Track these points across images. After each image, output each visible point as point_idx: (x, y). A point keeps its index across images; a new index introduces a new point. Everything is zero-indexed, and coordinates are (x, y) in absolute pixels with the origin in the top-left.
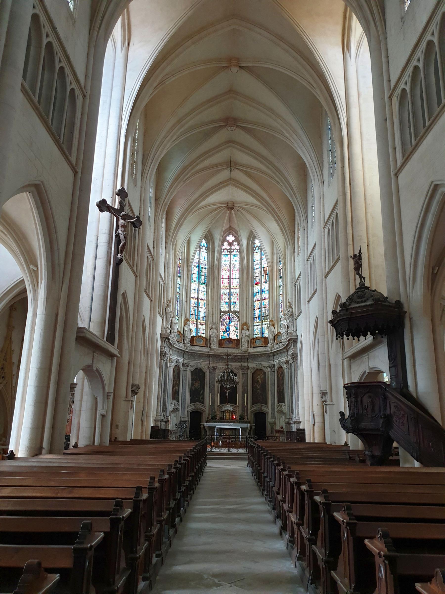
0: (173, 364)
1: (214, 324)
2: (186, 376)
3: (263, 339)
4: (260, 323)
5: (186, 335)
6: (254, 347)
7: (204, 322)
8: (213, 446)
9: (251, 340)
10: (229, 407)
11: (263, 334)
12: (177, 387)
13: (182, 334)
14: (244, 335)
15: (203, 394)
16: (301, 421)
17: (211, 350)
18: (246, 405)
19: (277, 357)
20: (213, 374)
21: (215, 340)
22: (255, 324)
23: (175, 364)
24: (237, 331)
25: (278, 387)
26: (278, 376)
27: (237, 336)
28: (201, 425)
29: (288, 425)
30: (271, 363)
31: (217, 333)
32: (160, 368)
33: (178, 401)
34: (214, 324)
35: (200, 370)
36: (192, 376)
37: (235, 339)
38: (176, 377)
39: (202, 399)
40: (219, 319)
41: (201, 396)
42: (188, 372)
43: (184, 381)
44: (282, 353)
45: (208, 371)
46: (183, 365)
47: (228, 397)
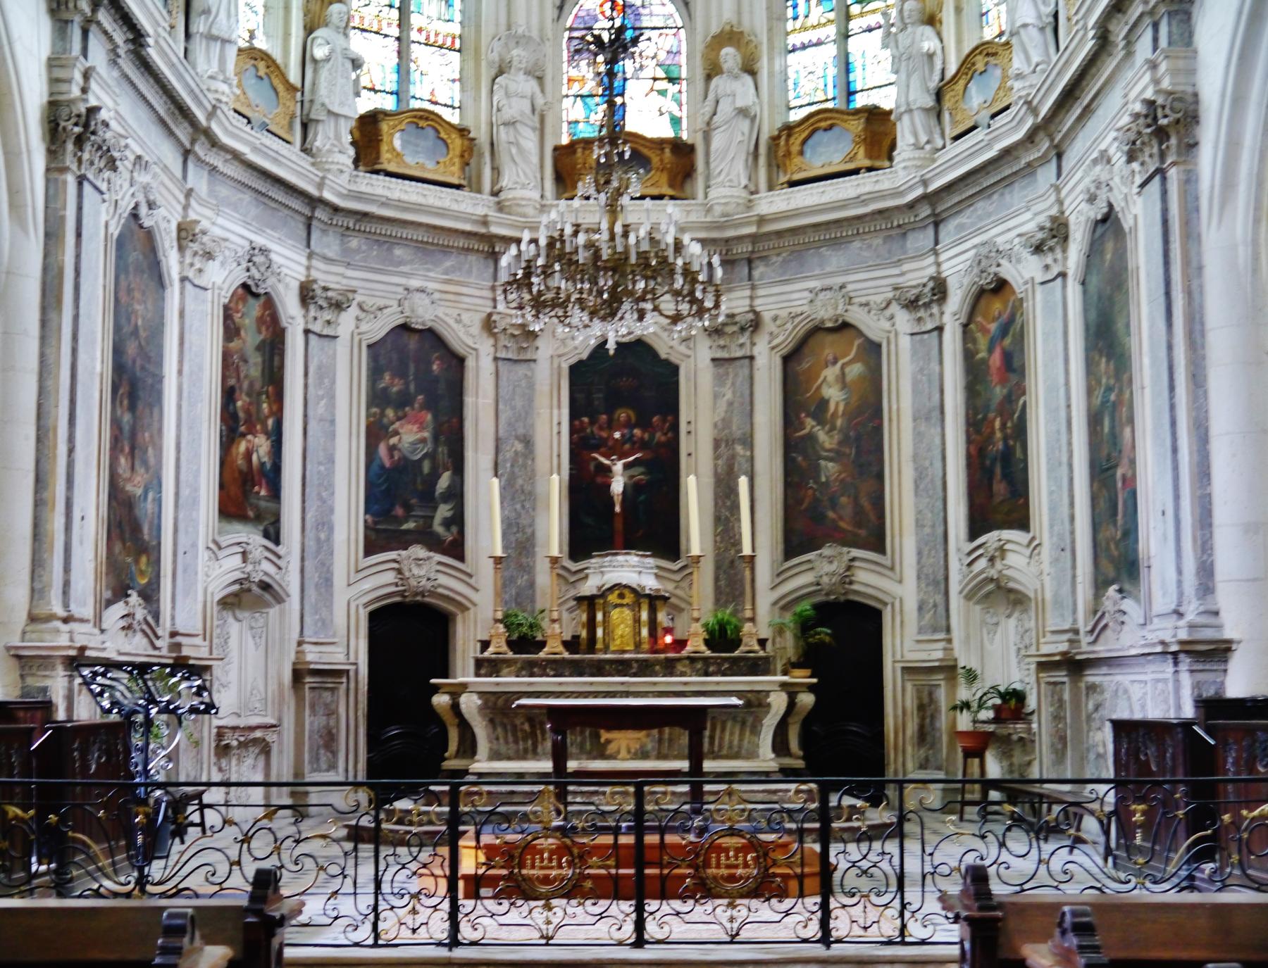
0: (222, 277)
1: (519, 40)
2: (328, 372)
3: (857, 126)
4: (831, 31)
5: (323, 91)
6: (793, 184)
7: (456, 29)
8: (475, 885)
9: (775, 139)
10: (631, 569)
11: (850, 94)
12: (262, 445)
13: (291, 88)
14: (725, 109)
15: (456, 495)
16: (1228, 634)
17: (500, 207)
18: (747, 550)
19: (961, 227)
20: (521, 370)
21: (529, 141)
22: (794, 40)
23: (240, 276)
24: (672, 89)
25: (975, 425)
26: (969, 356)
27: (676, 121)
28: (436, 689)
29: (1061, 676)
30: (917, 274)
31: (540, 101)
32: (52, 236)
33: (273, 534)
34: (519, 40)
35: (432, 338)
36: (375, 372)
37: (660, 143)
38: (254, 369)
39: (447, 523)
40: (550, 13)
41: (444, 511)
42: (342, 349)
43: (318, 410)
44: (1007, 182)
45: (485, 347)
46: (306, 295)
47: (624, 511)
